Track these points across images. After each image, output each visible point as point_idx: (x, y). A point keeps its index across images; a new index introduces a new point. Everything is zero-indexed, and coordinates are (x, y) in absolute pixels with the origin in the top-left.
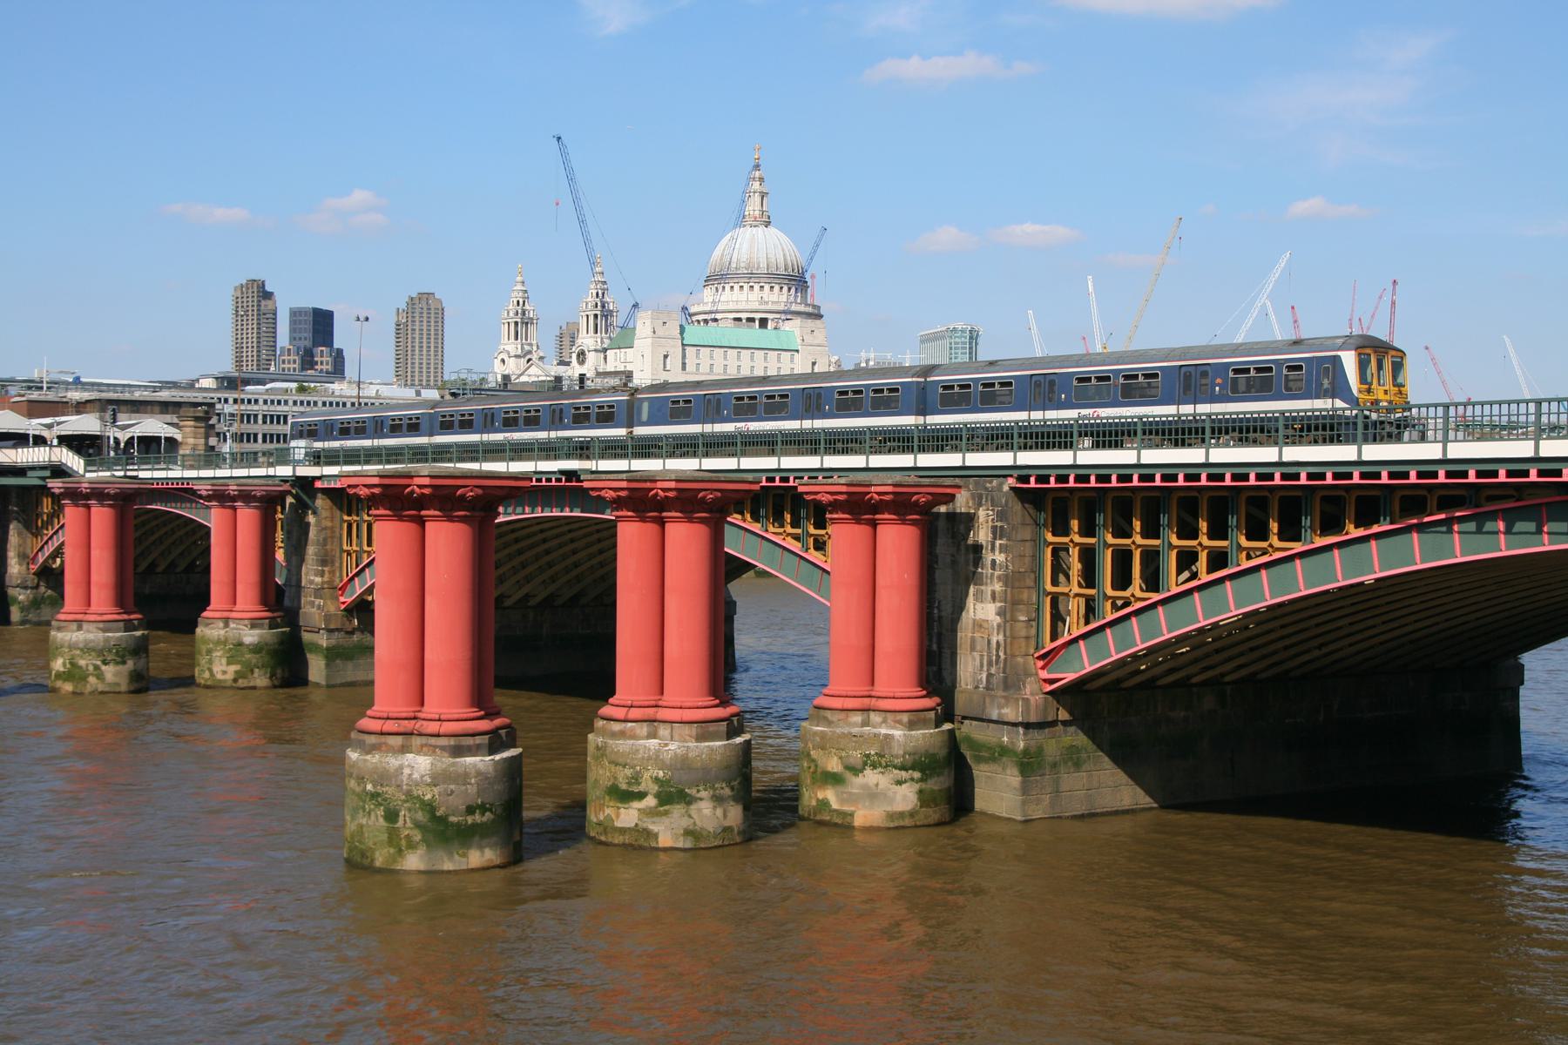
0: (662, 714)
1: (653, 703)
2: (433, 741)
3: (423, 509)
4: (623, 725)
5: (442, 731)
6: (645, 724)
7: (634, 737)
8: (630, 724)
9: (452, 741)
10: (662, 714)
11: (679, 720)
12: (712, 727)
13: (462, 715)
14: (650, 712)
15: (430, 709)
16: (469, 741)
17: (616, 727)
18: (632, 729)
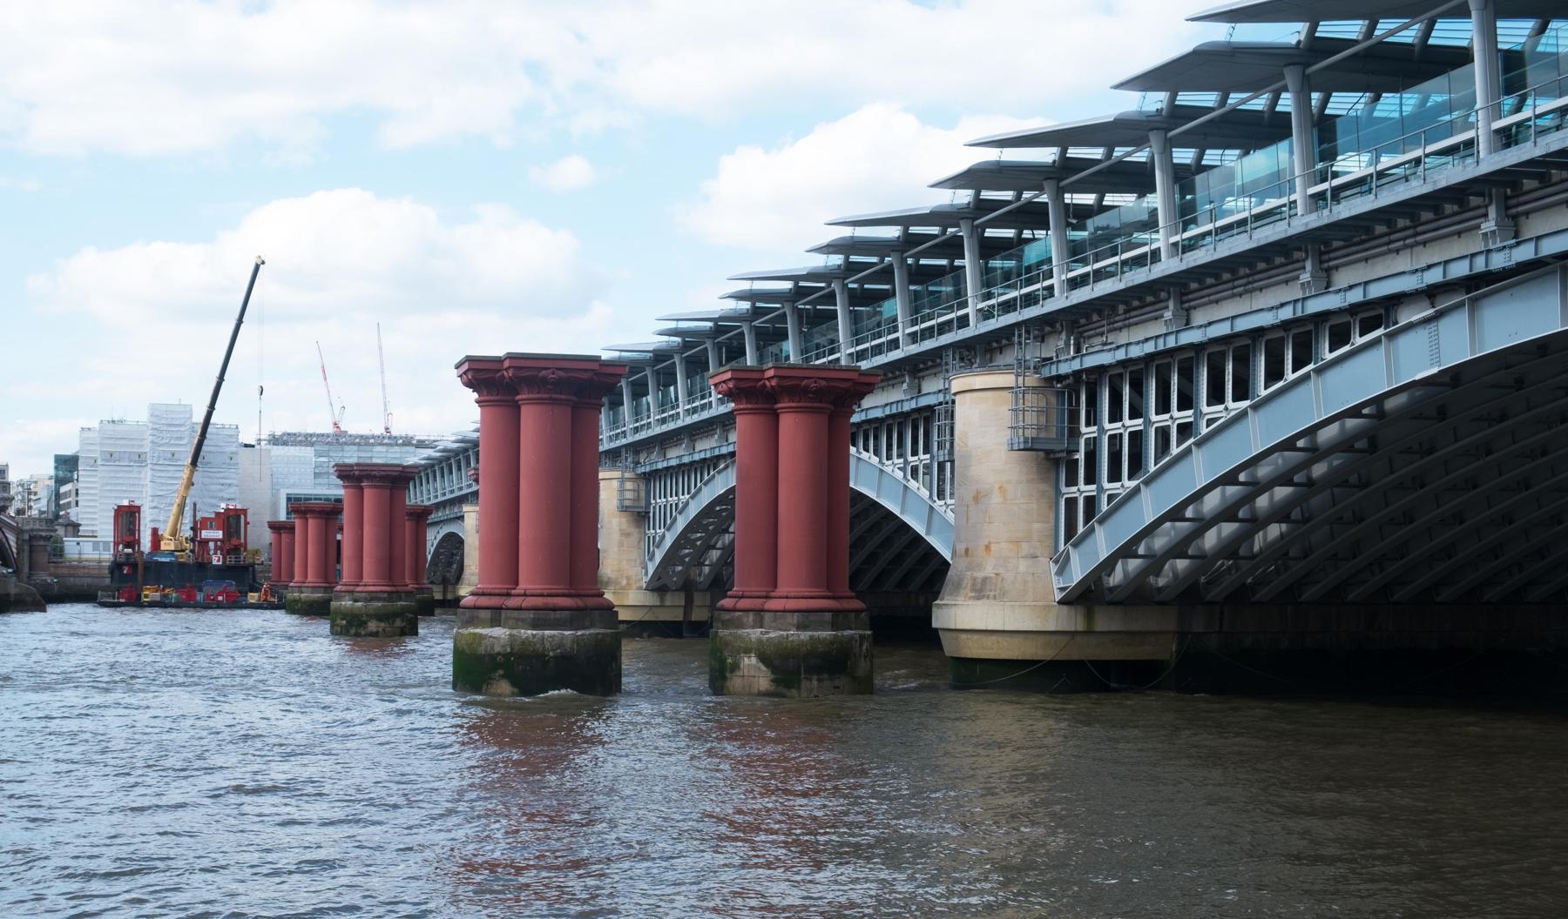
0: (771, 604)
1: (764, 594)
2: (515, 614)
3: (518, 394)
4: (732, 614)
5: (524, 605)
6: (751, 614)
7: (742, 626)
8: (738, 614)
9: (531, 615)
10: (771, 604)
11: (782, 608)
12: (813, 617)
13: (549, 591)
14: (757, 603)
15: (524, 585)
16: (552, 615)
17: (726, 616)
18: (739, 618)
